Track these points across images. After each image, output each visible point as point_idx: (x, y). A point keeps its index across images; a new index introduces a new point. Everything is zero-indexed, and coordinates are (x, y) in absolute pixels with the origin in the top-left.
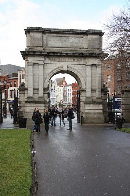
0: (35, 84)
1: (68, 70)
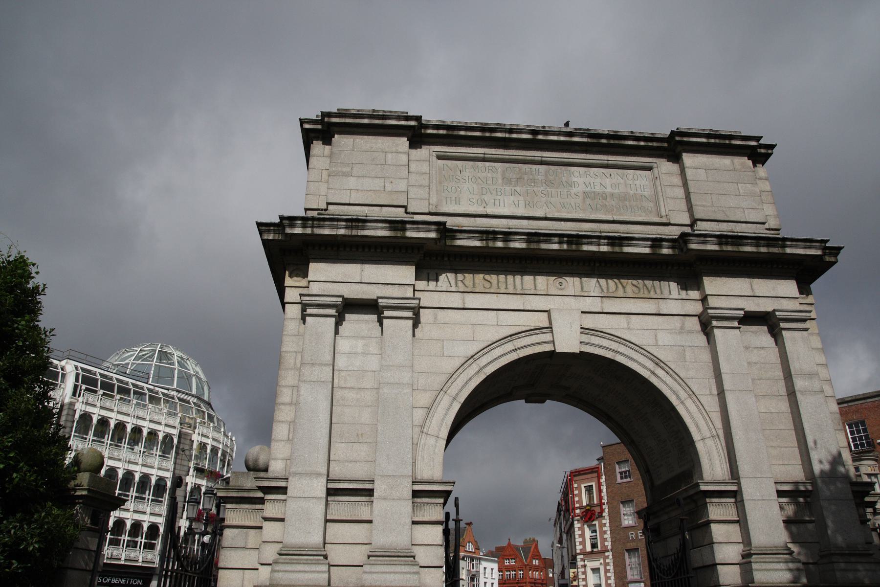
0: (339, 450)
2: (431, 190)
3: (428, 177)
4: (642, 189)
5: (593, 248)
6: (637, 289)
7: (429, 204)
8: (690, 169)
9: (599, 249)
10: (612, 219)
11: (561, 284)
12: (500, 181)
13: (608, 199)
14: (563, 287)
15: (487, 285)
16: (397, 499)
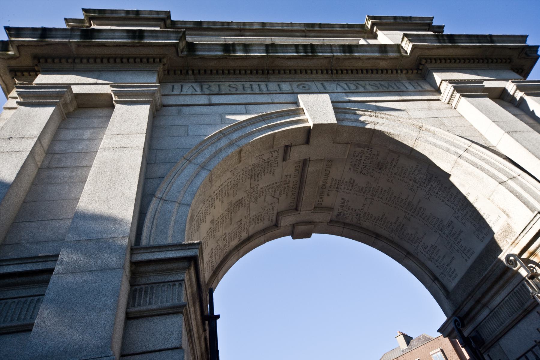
1: (345, 123)
14: (307, 88)
16: (97, 270)
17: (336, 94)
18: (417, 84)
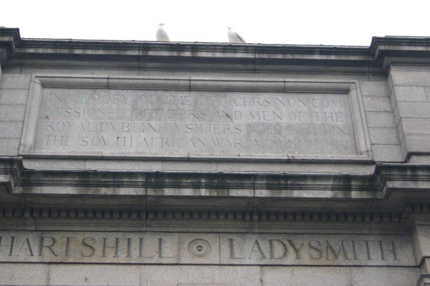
2: (25, 126)
3: (24, 110)
4: (335, 118)
5: (246, 193)
6: (318, 253)
7: (20, 144)
8: (401, 87)
9: (254, 193)
10: (285, 158)
11: (199, 248)
12: (128, 113)
13: (283, 133)
14: (202, 252)
15: (88, 252)
17: (245, 268)
18: (391, 248)
